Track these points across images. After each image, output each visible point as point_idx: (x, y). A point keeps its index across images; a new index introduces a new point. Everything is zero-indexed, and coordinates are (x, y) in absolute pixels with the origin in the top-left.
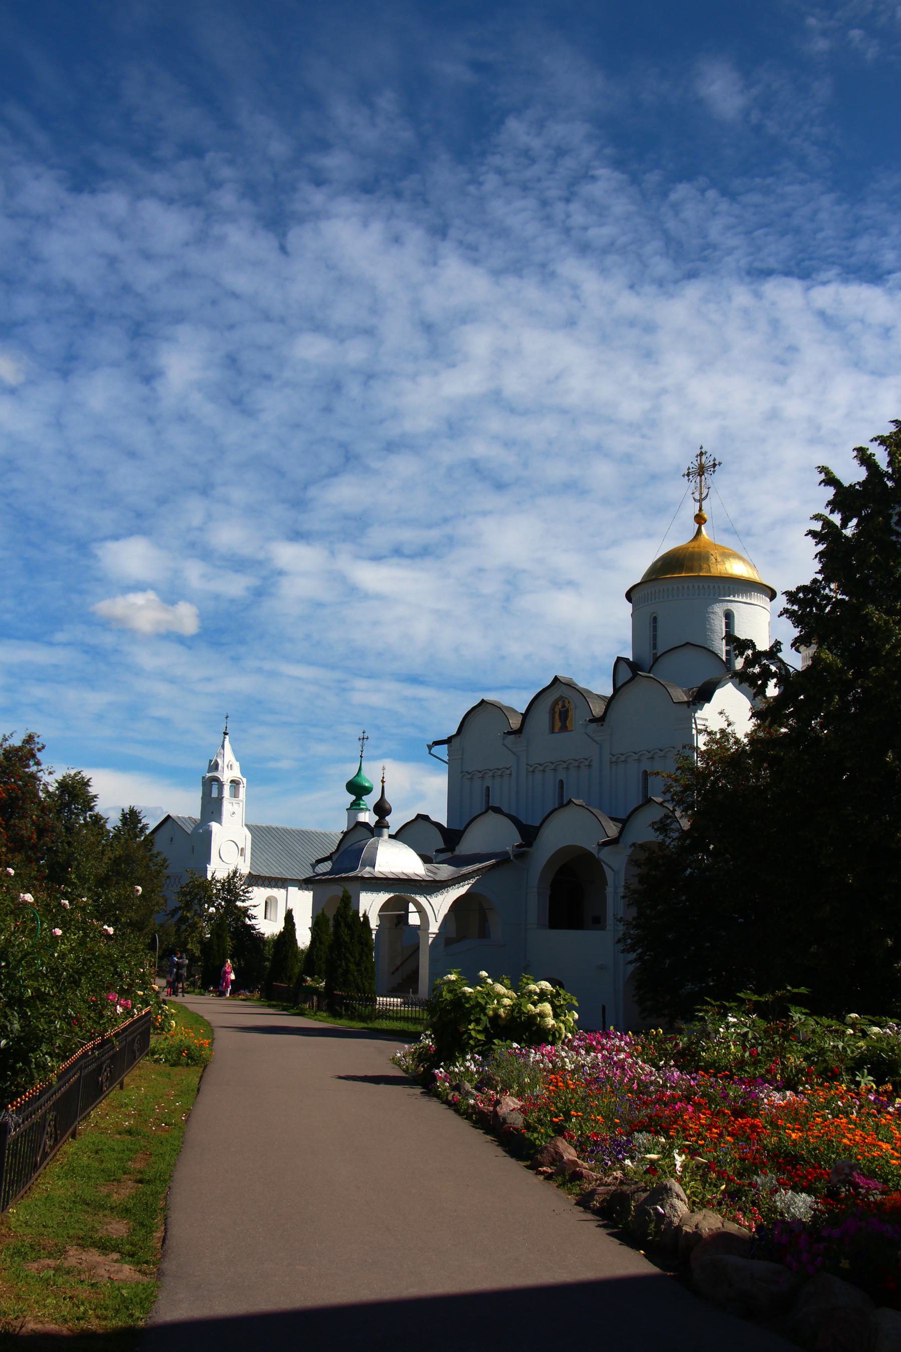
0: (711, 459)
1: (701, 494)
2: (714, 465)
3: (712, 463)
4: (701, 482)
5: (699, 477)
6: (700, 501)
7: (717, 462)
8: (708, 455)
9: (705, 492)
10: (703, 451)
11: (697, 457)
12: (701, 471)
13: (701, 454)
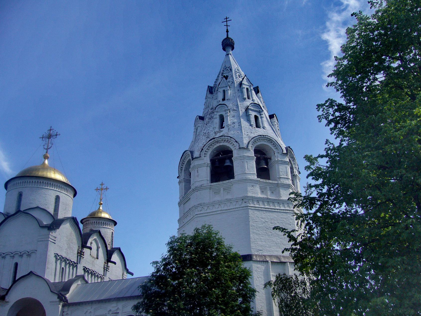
0: (55, 132)
1: (48, 146)
2: (56, 135)
3: (55, 134)
4: (49, 141)
5: (48, 139)
6: (47, 149)
7: (58, 134)
8: (54, 130)
9: (50, 145)
10: (52, 128)
11: (48, 131)
12: (50, 136)
13: (50, 130)
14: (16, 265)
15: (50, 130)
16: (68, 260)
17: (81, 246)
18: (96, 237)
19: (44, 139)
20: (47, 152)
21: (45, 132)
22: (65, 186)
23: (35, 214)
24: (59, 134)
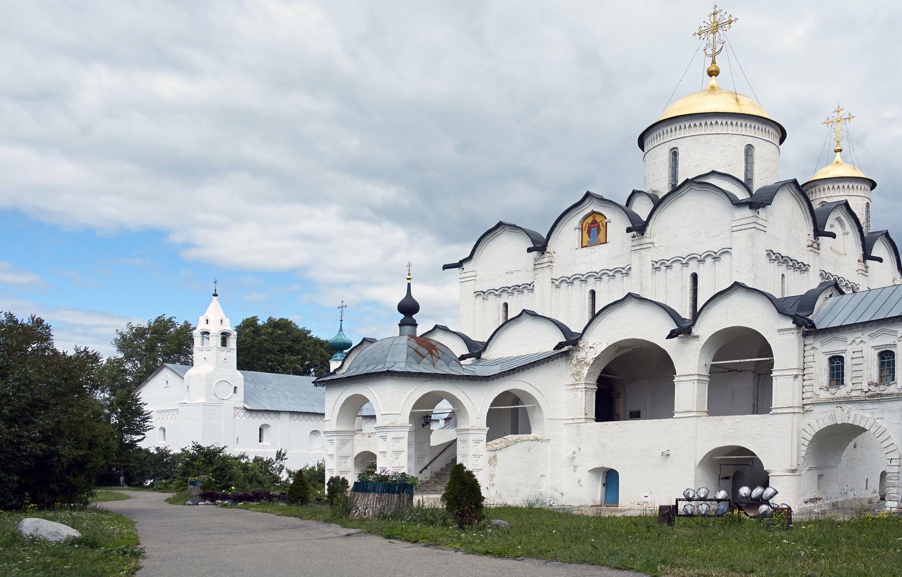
0: (727, 16)
1: (714, 48)
3: (727, 20)
7: (733, 19)
10: (717, 9)
11: (710, 16)
12: (715, 28)
13: (714, 14)
14: (695, 277)
15: (714, 14)
16: (792, 260)
17: (812, 233)
18: (840, 214)
19: (703, 35)
20: (714, 62)
21: (703, 19)
22: (763, 123)
23: (713, 181)
24: (736, 19)
